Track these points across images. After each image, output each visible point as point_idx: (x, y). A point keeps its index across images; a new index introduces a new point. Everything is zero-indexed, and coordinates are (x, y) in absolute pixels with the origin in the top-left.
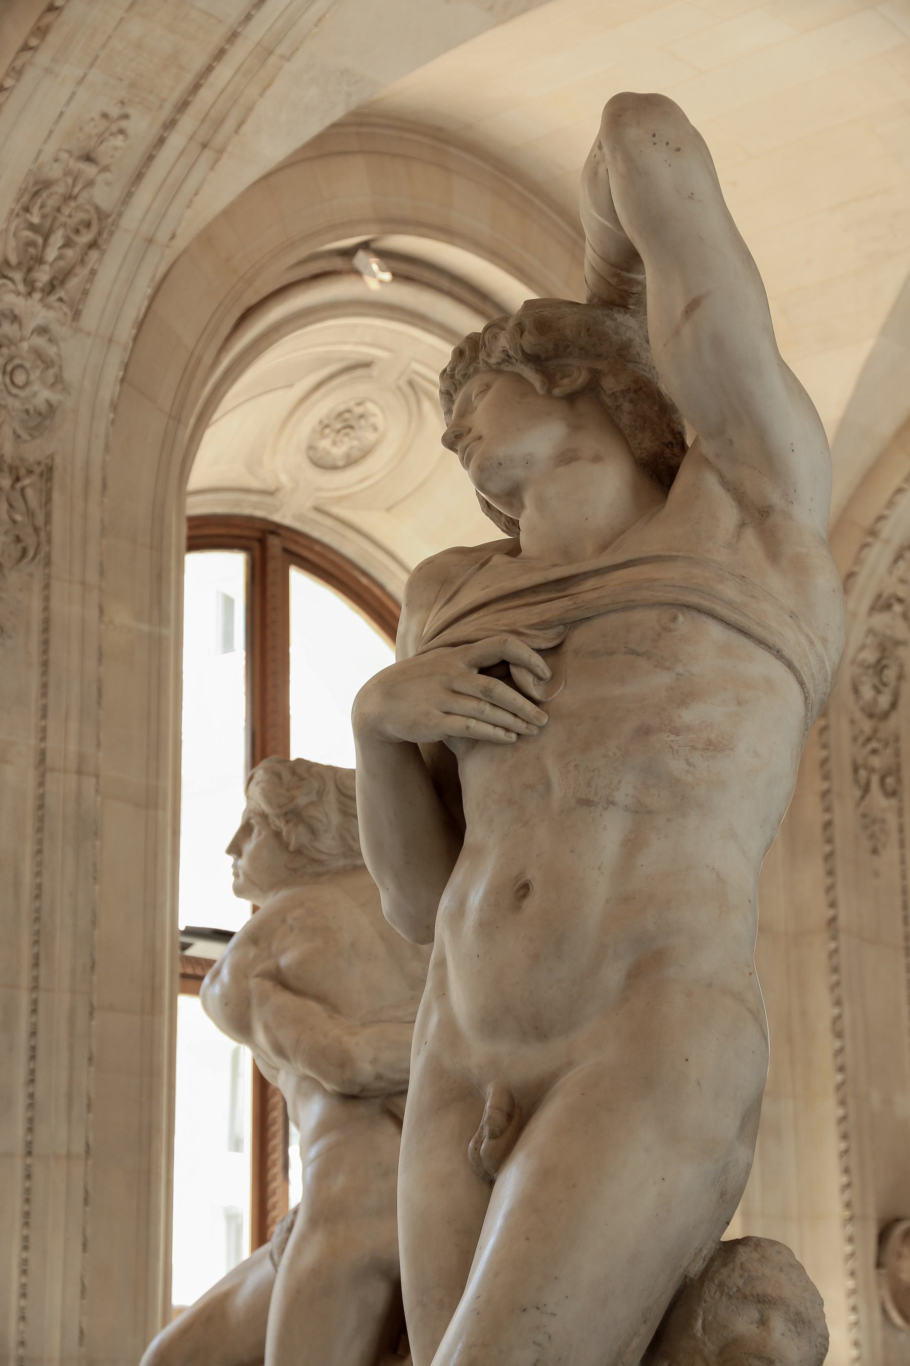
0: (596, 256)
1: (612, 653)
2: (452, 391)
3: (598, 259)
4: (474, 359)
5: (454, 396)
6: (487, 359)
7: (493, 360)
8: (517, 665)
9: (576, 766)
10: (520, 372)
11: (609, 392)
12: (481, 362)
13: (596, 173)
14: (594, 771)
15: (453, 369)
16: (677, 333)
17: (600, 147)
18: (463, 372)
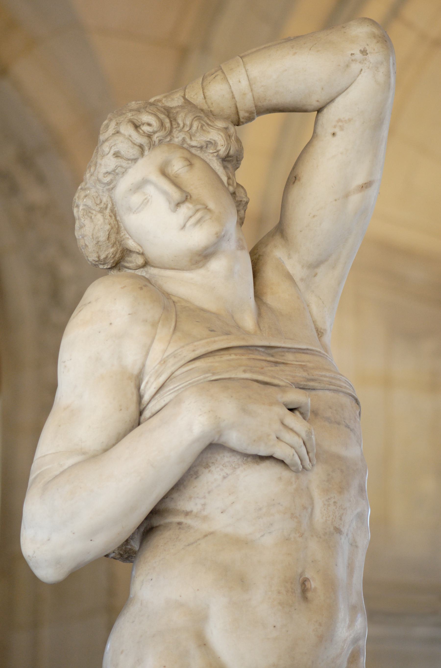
0: (251, 94)
1: (339, 424)
2: (146, 148)
3: (249, 96)
4: (171, 132)
5: (146, 153)
6: (188, 140)
7: (194, 143)
8: (302, 414)
9: (335, 502)
10: (208, 161)
11: (238, 199)
12: (180, 138)
13: (348, 66)
14: (344, 509)
15: (155, 132)
16: (347, 196)
17: (364, 52)
18: (162, 138)
